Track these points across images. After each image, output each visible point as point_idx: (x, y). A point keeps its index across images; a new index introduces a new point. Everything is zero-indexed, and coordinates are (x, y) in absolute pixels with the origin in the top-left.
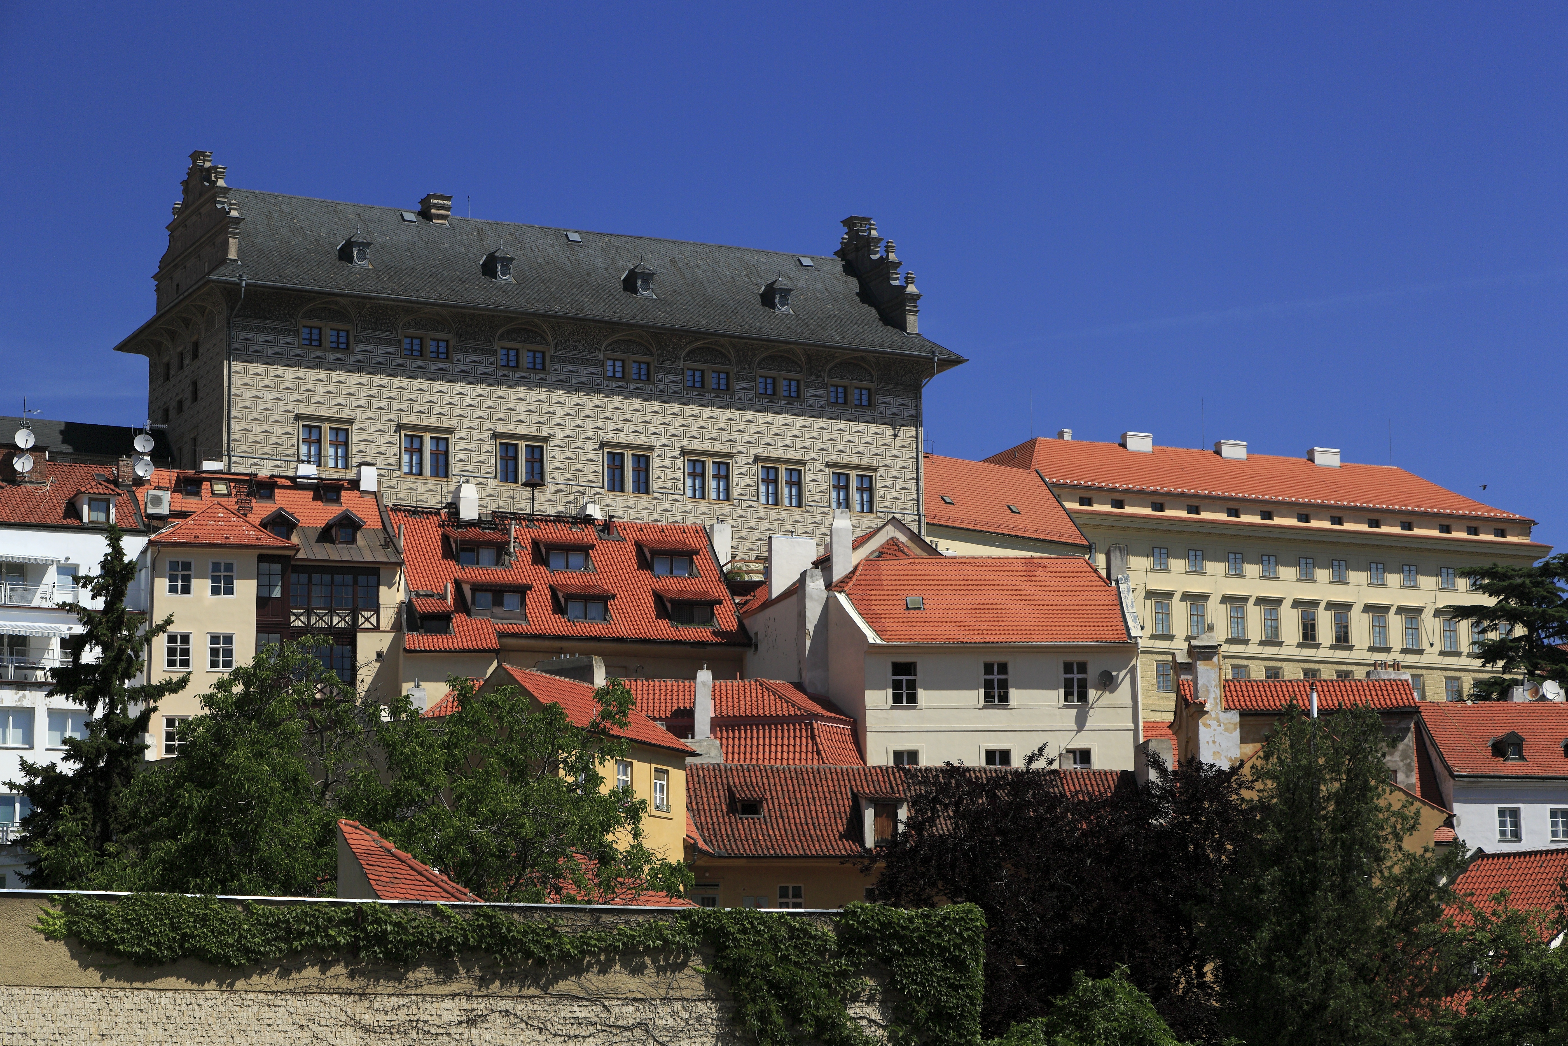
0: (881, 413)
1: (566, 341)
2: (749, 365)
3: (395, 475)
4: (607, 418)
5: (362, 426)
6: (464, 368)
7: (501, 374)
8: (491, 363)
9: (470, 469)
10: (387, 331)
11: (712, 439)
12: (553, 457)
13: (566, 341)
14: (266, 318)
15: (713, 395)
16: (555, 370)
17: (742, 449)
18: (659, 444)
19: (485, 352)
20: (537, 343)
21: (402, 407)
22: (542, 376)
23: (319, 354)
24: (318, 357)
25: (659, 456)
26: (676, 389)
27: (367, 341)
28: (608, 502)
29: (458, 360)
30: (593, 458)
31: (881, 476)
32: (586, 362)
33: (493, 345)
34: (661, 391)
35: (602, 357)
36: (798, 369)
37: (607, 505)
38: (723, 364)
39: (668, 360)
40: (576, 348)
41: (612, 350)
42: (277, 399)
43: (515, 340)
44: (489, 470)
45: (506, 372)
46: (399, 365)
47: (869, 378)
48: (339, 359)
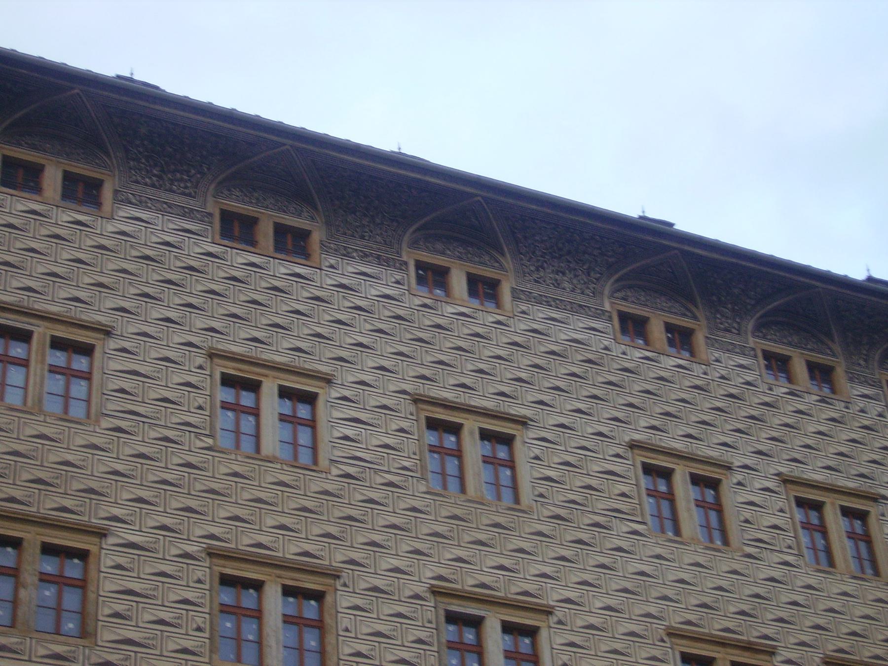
1: (538, 270)
2: (865, 360)
3: (200, 444)
5: (127, 345)
7: (417, 301)
8: (398, 282)
9: (367, 456)
18: (737, 464)
20: (484, 264)
26: (749, 379)
27: (141, 204)
33: (399, 253)
34: (722, 377)
35: (607, 306)
38: (822, 353)
39: (727, 330)
40: (557, 285)
41: (625, 299)
43: (443, 253)
44: (406, 464)
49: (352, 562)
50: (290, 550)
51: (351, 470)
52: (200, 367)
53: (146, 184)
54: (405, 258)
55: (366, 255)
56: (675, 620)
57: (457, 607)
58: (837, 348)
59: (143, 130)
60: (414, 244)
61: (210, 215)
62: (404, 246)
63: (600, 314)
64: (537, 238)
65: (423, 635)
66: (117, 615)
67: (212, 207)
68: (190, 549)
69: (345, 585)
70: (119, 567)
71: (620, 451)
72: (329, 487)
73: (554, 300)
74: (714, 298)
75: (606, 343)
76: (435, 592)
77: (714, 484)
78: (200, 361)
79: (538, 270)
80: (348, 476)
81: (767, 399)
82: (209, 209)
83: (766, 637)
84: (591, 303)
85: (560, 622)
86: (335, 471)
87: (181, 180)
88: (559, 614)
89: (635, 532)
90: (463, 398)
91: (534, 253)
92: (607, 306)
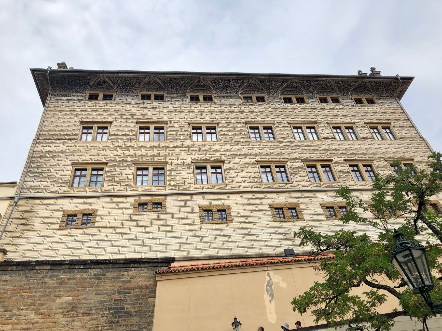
1: (221, 91)
9: (177, 137)
12: (221, 130)
14: (70, 92)
17: (320, 121)
23: (96, 102)
25: (277, 126)
27: (121, 97)
28: (254, 144)
34: (272, 105)
35: (240, 96)
36: (336, 94)
37: (253, 145)
39: (272, 95)
40: (226, 93)
43: (197, 93)
47: (371, 95)
49: (171, 159)
50: (155, 160)
52: (134, 126)
53: (123, 93)
54: (187, 95)
55: (177, 97)
56: (259, 158)
57: (198, 165)
58: (304, 92)
59: (119, 81)
60: (190, 92)
64: (219, 84)
65: (189, 172)
66: (109, 180)
67: (139, 94)
68: (129, 163)
69: (169, 164)
71: (244, 125)
72: (166, 145)
74: (268, 88)
75: (240, 103)
76: (192, 162)
77: (271, 128)
79: (221, 91)
83: (285, 158)
84: (236, 96)
87: (131, 90)
88: (226, 162)
90: (201, 121)
91: (219, 88)
92: (240, 96)
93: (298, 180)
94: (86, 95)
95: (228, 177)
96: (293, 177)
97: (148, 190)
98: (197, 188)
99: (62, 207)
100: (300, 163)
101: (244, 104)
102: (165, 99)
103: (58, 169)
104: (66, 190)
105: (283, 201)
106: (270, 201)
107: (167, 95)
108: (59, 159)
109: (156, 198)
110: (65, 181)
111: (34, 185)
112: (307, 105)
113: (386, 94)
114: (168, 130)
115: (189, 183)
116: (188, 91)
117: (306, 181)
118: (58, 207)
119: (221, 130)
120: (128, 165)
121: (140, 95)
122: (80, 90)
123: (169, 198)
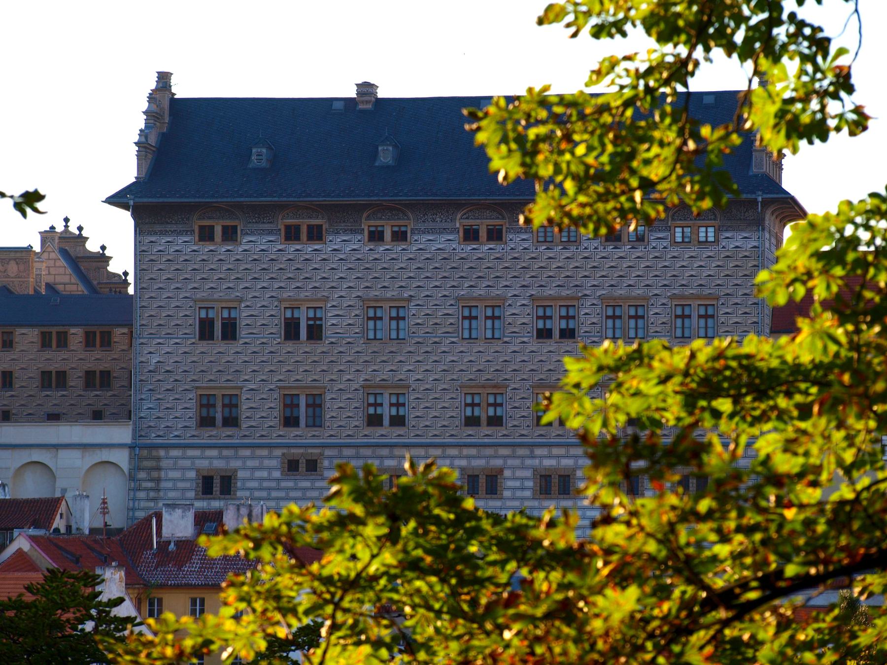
0: (723, 247)
1: (424, 215)
3: (275, 342)
4: (462, 277)
5: (248, 304)
6: (336, 247)
7: (367, 249)
8: (359, 241)
10: (268, 223)
11: (559, 286)
13: (424, 215)
14: (167, 223)
15: (560, 247)
16: (416, 240)
17: (588, 292)
18: (510, 295)
19: (353, 231)
20: (399, 219)
21: (282, 285)
22: (404, 247)
23: (212, 248)
24: (211, 251)
26: (525, 246)
27: (252, 233)
28: (462, 349)
29: (330, 241)
30: (450, 312)
31: (723, 304)
32: (444, 231)
34: (512, 249)
35: (458, 225)
40: (434, 220)
41: (467, 218)
42: (178, 288)
43: (381, 219)
44: (357, 331)
45: (372, 247)
46: (280, 250)
47: (713, 217)
48: (228, 251)
49: (332, 380)
51: (333, 340)
52: (276, 306)
54: (363, 227)
60: (368, 218)
61: (280, 230)
62: (363, 220)
63: (455, 231)
66: (247, 417)
70: (247, 399)
71: (452, 302)
72: (324, 350)
73: (431, 229)
75: (454, 246)
78: (276, 304)
80: (332, 343)
81: (533, 255)
82: (279, 227)
84: (449, 225)
85: (413, 390)
86: (327, 342)
89: (453, 342)
93: (515, 423)
94: (194, 231)
95: (412, 416)
96: (510, 417)
97: (300, 436)
98: (366, 435)
99: (193, 463)
100: (528, 389)
101: (462, 249)
102: (324, 238)
103: (177, 396)
104: (194, 433)
105: (481, 463)
106: (463, 463)
107: (328, 227)
108: (176, 378)
109: (310, 451)
110: (190, 418)
111: (152, 424)
112: (577, 249)
113: (745, 213)
114: (330, 314)
115: (356, 426)
116: (365, 215)
117: (528, 426)
118: (187, 463)
119: (414, 315)
120: (271, 390)
121: (283, 226)
122: (183, 220)
123: (328, 452)
